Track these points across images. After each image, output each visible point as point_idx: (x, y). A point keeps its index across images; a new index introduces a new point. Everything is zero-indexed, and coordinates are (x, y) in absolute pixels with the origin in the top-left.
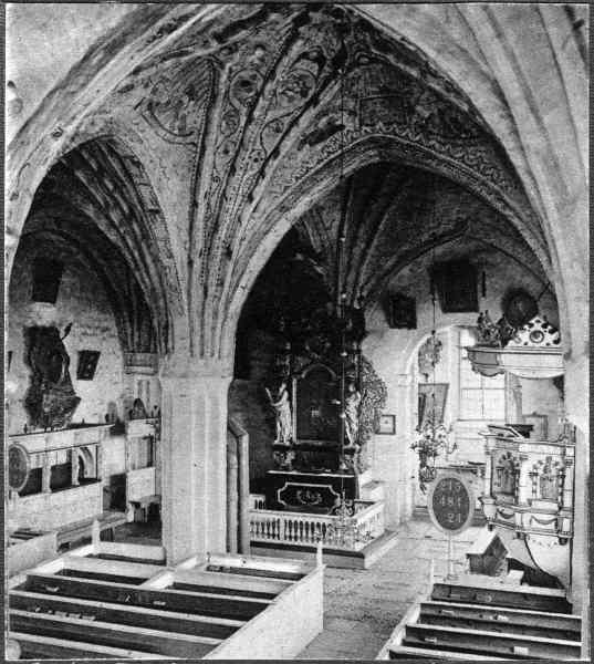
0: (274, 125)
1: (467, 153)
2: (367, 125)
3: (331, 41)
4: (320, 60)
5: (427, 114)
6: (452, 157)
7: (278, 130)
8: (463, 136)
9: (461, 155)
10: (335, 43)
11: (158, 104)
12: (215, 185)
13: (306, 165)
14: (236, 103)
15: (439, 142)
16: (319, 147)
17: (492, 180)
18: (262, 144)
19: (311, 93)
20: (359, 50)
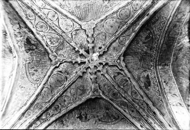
0: (133, 94)
1: (157, 34)
2: (151, 67)
3: (114, 69)
4: (119, 73)
5: (146, 48)
6: (159, 39)
7: (136, 93)
8: (151, 36)
9: (158, 36)
10: (115, 68)
11: (101, 118)
12: (141, 121)
13: (156, 90)
14: (120, 99)
15: (155, 44)
16: (152, 84)
17: (164, 23)
18: (137, 100)
19: (128, 79)
20: (114, 62)
